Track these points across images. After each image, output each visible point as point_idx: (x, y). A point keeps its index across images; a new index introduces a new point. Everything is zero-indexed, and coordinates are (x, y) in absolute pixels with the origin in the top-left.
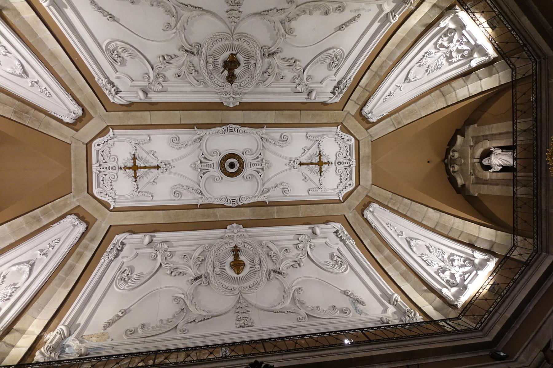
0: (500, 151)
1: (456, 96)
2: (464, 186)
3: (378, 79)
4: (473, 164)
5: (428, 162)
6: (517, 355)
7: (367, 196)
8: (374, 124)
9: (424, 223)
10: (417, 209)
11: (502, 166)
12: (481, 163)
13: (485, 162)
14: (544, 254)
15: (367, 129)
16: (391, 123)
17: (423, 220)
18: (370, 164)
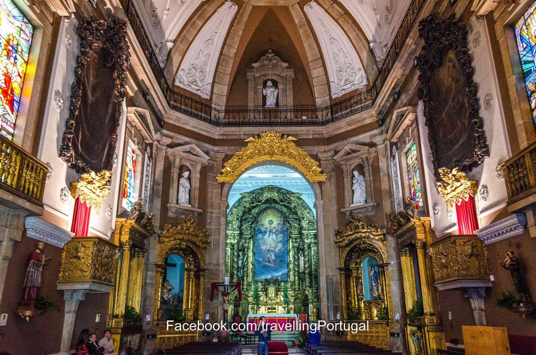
0: (276, 95)
1: (314, 69)
2: (253, 68)
3: (336, 17)
4: (268, 75)
5: (270, 40)
7: (244, 2)
8: (302, 9)
9: (226, 47)
10: (235, 40)
11: (266, 95)
12: (268, 80)
13: (269, 83)
15: (298, 3)
16: (302, 21)
17: (228, 45)
18: (269, 5)
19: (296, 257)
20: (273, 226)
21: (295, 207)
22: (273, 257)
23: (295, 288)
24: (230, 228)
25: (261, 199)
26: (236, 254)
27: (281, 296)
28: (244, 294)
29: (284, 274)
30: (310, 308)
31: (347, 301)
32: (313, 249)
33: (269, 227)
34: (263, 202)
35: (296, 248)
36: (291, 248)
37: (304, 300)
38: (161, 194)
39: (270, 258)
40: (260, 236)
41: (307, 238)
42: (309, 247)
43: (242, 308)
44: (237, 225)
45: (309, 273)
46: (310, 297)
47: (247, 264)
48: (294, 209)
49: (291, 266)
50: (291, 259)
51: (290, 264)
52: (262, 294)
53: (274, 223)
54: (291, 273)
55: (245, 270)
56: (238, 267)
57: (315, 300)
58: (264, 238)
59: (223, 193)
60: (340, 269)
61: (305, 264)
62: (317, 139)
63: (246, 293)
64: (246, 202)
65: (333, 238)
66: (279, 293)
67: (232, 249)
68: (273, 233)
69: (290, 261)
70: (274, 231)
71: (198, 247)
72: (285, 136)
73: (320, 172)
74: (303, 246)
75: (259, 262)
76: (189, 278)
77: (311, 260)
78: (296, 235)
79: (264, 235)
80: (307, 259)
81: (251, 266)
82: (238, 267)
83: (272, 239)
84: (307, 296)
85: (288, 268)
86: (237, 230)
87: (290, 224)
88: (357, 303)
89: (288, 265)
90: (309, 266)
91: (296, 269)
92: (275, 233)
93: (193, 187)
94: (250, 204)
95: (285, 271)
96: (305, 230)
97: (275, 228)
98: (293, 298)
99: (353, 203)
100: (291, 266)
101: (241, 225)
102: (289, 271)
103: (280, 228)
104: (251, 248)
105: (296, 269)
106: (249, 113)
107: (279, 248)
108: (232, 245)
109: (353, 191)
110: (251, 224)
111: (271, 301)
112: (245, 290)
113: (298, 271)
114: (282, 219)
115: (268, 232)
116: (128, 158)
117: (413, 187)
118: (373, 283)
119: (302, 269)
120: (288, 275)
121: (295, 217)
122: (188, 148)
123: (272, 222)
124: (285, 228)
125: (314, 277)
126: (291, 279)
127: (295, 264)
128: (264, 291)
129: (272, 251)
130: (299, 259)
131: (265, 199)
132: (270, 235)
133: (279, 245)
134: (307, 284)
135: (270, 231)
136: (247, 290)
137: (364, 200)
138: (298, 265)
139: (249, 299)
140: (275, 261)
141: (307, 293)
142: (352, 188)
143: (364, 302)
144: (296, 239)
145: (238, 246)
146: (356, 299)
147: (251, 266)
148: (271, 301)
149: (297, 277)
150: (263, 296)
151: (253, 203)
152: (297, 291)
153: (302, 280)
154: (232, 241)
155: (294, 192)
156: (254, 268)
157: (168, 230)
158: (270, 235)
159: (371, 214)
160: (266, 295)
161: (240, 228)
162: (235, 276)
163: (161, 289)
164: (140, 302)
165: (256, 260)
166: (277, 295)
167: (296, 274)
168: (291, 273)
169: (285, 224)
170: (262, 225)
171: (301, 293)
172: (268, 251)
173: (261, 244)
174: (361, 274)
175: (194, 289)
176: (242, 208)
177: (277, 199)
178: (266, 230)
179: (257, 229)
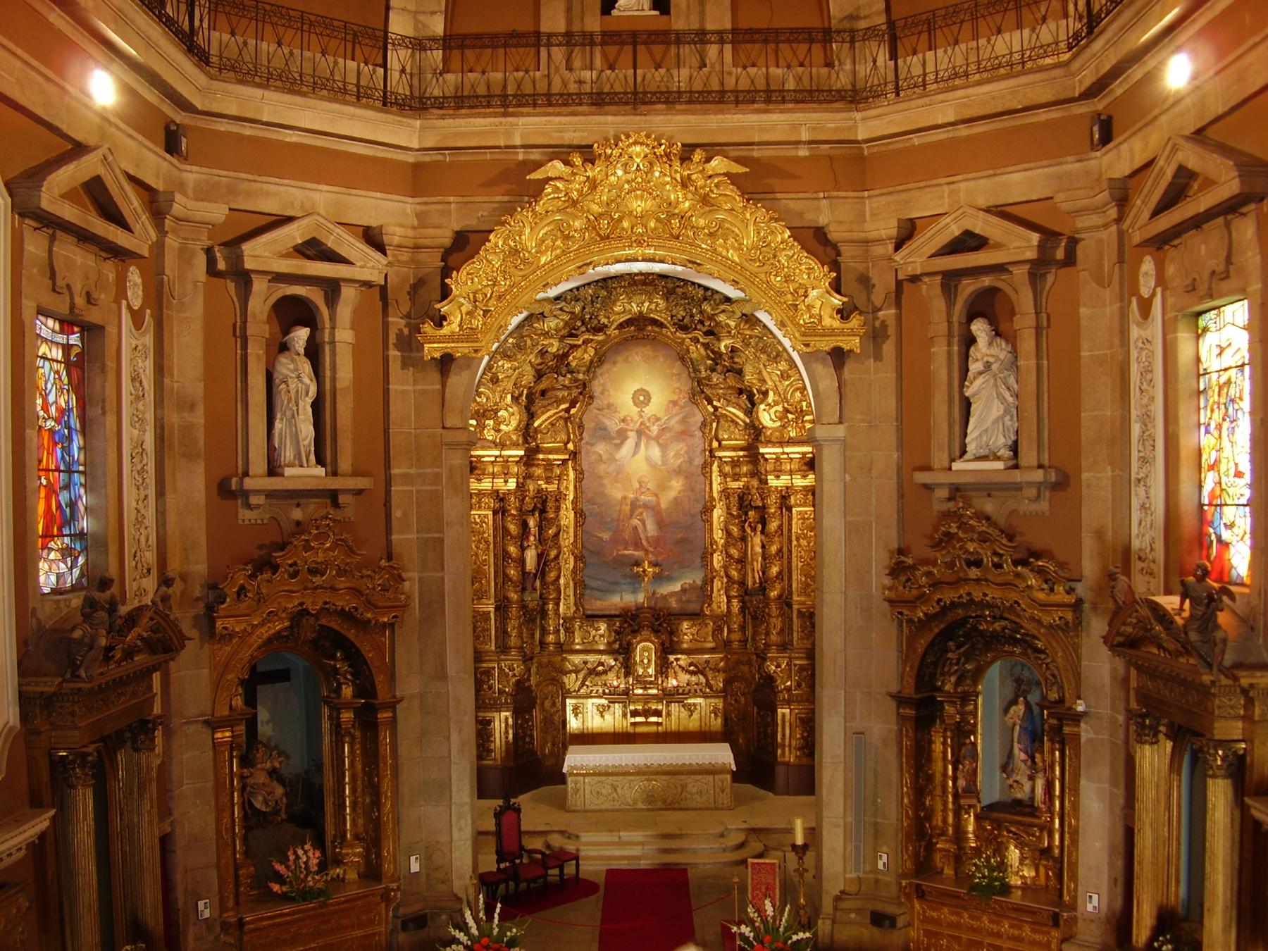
6: (194, 168)
14: (418, 123)
19: (735, 530)
20: (649, 410)
21: (734, 350)
22: (651, 529)
24: (489, 435)
26: (512, 528)
29: (693, 587)
31: (916, 811)
32: (800, 513)
33: (636, 418)
35: (734, 500)
36: (715, 495)
38: (201, 443)
39: (640, 529)
40: (601, 448)
41: (778, 473)
44: (514, 423)
45: (780, 596)
47: (557, 557)
48: (732, 358)
49: (717, 560)
50: (718, 535)
51: (715, 551)
52: (613, 663)
53: (654, 399)
54: (717, 584)
56: (524, 574)
58: (618, 456)
59: (447, 395)
60: (900, 700)
62: (831, 158)
64: (546, 334)
65: (878, 580)
66: (672, 658)
67: (500, 512)
68: (649, 438)
69: (713, 542)
70: (655, 429)
71: (363, 625)
72: (698, 156)
73: (839, 311)
76: (338, 732)
77: (790, 551)
78: (734, 449)
79: (618, 446)
80: (774, 549)
82: (524, 574)
83: (648, 459)
86: (515, 445)
88: (950, 820)
89: (706, 556)
91: (734, 574)
92: (657, 439)
93: (328, 386)
94: (562, 339)
96: (769, 442)
97: (658, 419)
99: (964, 452)
100: (717, 560)
101: (532, 416)
102: (708, 581)
103: (678, 418)
104: (571, 497)
105: (734, 574)
106: (543, 51)
107: (672, 494)
108: (499, 497)
109: (967, 404)
113: (742, 583)
114: (685, 385)
115: (632, 435)
116: (45, 369)
117: (1211, 468)
118: (1016, 751)
119: (753, 579)
120: (704, 591)
122: (297, 234)
127: (729, 555)
129: (646, 506)
130: (743, 539)
132: (637, 445)
135: (640, 433)
137: (1010, 443)
138: (742, 561)
140: (656, 542)
142: (962, 386)
143: (977, 817)
144: (735, 463)
146: (950, 806)
147: (568, 563)
148: (645, 688)
149: (736, 605)
153: (754, 618)
154: (499, 483)
157: (242, 588)
158: (637, 445)
159: (1035, 507)
161: (527, 432)
162: (514, 610)
163: (242, 777)
164: (160, 906)
167: (733, 593)
170: (609, 406)
172: (634, 505)
174: (975, 717)
175: (359, 766)
176: (532, 358)
179: (589, 425)
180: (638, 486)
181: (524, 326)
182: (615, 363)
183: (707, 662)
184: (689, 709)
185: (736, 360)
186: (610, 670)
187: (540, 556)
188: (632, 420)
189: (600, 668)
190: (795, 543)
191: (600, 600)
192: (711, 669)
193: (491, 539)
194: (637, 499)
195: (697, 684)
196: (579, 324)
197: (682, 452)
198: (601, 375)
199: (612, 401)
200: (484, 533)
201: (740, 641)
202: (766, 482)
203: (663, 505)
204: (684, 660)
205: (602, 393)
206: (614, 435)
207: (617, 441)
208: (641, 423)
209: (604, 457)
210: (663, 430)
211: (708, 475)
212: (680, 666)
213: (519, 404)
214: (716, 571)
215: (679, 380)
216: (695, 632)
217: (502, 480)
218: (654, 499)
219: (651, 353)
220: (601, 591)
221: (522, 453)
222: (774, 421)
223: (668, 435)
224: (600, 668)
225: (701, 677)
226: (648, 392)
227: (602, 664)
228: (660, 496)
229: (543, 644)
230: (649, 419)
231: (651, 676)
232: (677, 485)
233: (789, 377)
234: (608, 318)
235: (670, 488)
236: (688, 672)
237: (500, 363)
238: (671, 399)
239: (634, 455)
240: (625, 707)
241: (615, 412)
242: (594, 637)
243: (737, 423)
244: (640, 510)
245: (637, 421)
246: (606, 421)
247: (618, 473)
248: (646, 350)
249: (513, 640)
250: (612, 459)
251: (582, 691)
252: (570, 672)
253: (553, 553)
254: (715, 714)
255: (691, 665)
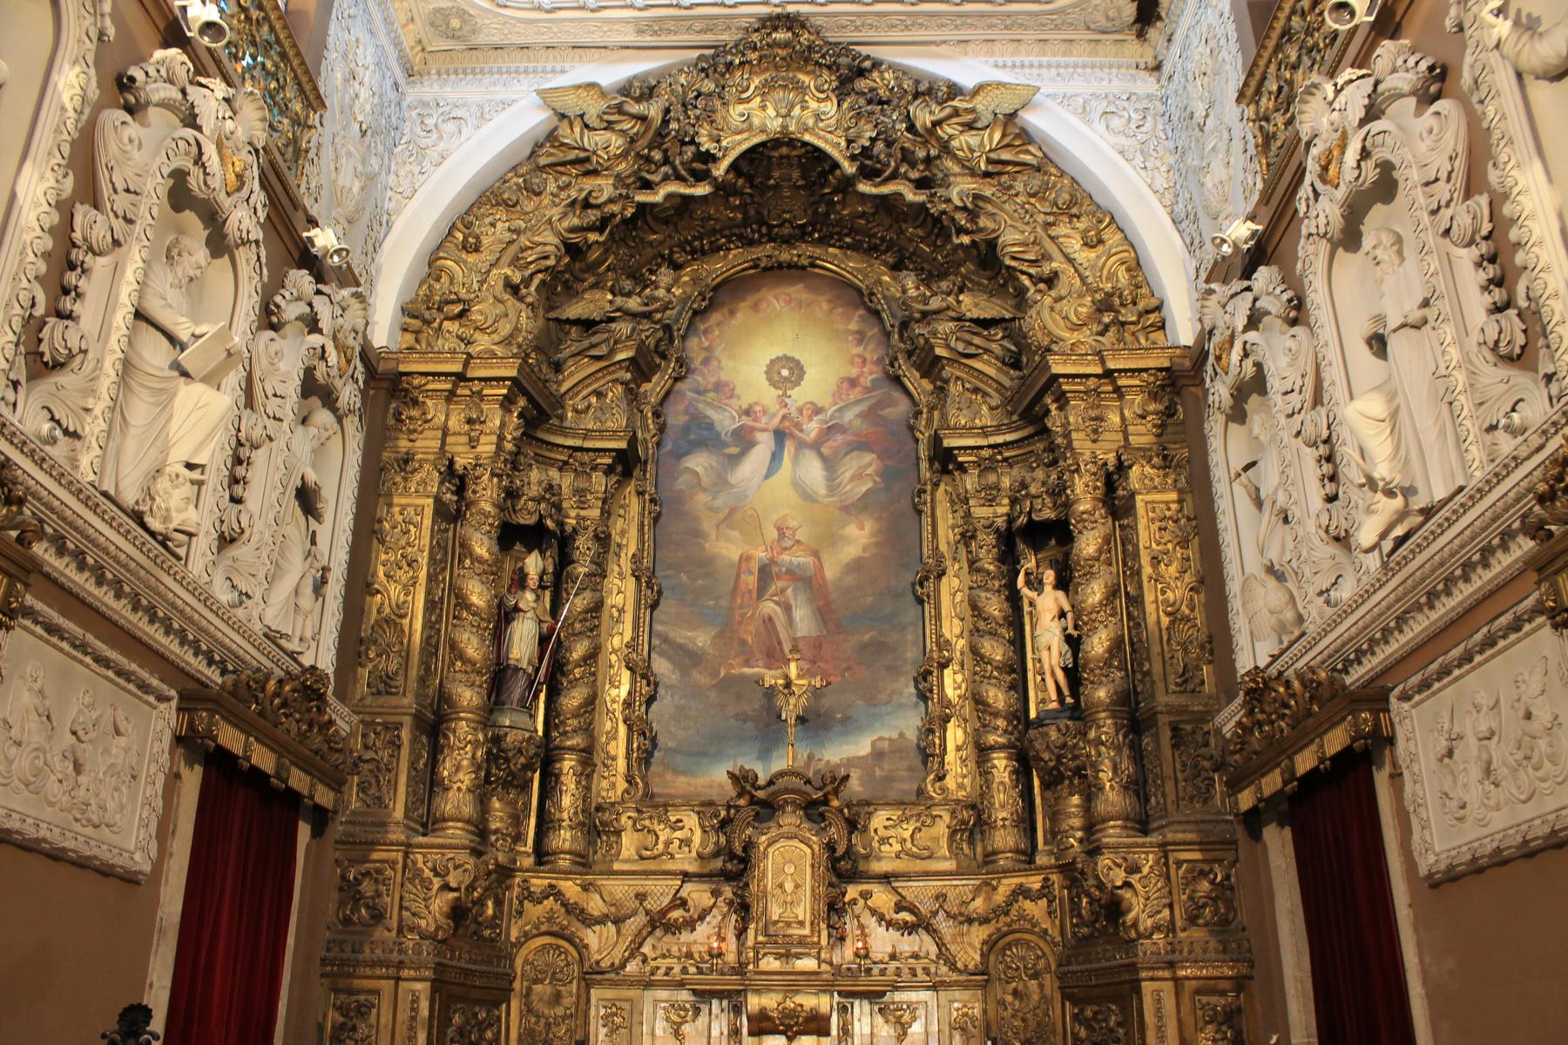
20: (800, 395)
22: (804, 620)
23: (990, 857)
25: (707, 145)
27: (871, 922)
28: (553, 892)
29: (898, 747)
30: (1149, 1018)
33: (773, 406)
34: (720, 170)
37: (1077, 948)
40: (699, 463)
42: (1116, 503)
43: (529, 1009)
44: (505, 329)
46: (1141, 909)
48: (973, 215)
49: (952, 684)
50: (952, 628)
51: (943, 666)
52: (707, 900)
53: (811, 374)
54: (955, 735)
55: (572, 700)
57: (1197, 934)
61: (1073, 643)
63: (570, 888)
67: (450, 515)
68: (801, 445)
69: (943, 644)
70: (812, 428)
74: (1059, 492)
75: (687, 658)
79: (735, 460)
80: (1094, 593)
81: (626, 676)
82: (499, 676)
84: (1113, 909)
85: (923, 696)
87: (930, 366)
90: (1116, 646)
92: (816, 446)
95: (907, 724)
97: (818, 411)
98: (979, 934)
100: (952, 684)
102: (935, 725)
103: (857, 409)
108: (458, 481)
110: (641, 368)
111: (786, 956)
112: (564, 862)
114: (873, 352)
115: (765, 443)
120: (928, 755)
121: (975, 313)
123: (798, 370)
124: (900, 408)
125: (1175, 729)
126: (950, 782)
128: (727, 876)
129: (793, 574)
131: (736, 145)
132: (776, 457)
133: (852, 530)
134: (1112, 797)
135: (780, 436)
136: (583, 863)
139: (592, 937)
140: (817, 644)
141: (1119, 876)
145: (512, 494)
148: (786, 956)
150: (714, 919)
151: (647, 185)
152: (1006, 872)
155: (967, 80)
156: (650, 700)
158: (776, 457)
160: (743, 909)
162: (464, 734)
165: (665, 639)
166: (834, 909)
167: (992, 739)
168: (955, 735)
169: (897, 380)
170: (718, 387)
171: (1045, 891)
172: (766, 573)
173: (708, 526)
176: (555, 213)
177: (833, 145)
178: (745, 420)
179: (676, 417)
180: (775, 534)
181: (542, 146)
182: (732, 313)
183: (941, 897)
184: (898, 1021)
185: (983, 222)
186: (701, 918)
187: (543, 640)
188: (765, 412)
189: (676, 914)
190: (1147, 570)
191: (684, 773)
192: (949, 915)
193: (424, 560)
194: (773, 562)
195: (916, 956)
196: (657, 155)
197: (869, 471)
198: (705, 332)
199: (724, 377)
200: (408, 544)
201: (1017, 851)
202: (1069, 446)
203: (831, 572)
204: (882, 898)
205: (706, 361)
206: (728, 439)
207: (734, 450)
208: (784, 417)
209: (705, 481)
210: (831, 430)
211: (927, 509)
212: (874, 912)
213: (521, 299)
214: (949, 704)
215: (860, 342)
216: (907, 835)
217: (464, 439)
218: (810, 560)
219: (805, 296)
220: (690, 754)
221: (513, 373)
222: (1075, 328)
223: (839, 439)
224: (676, 914)
225: (927, 939)
226: (798, 363)
227: (683, 903)
228: (825, 557)
229: (542, 855)
230: (800, 411)
231: (801, 924)
232: (858, 537)
233: (1101, 241)
234: (718, 141)
235: (846, 540)
236: (889, 924)
237: (487, 220)
238: (844, 374)
239: (767, 476)
240: (737, 1010)
241: (731, 397)
242: (668, 843)
243: (985, 394)
244: (780, 584)
245: (774, 415)
246: (711, 413)
247: (733, 511)
248: (797, 291)
249: (457, 798)
250: (722, 482)
251: (628, 968)
252: (601, 920)
253: (579, 650)
254: (963, 1030)
255: (899, 908)
